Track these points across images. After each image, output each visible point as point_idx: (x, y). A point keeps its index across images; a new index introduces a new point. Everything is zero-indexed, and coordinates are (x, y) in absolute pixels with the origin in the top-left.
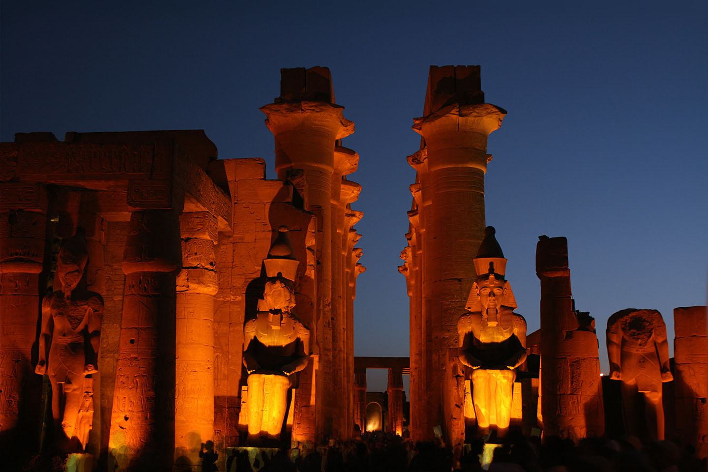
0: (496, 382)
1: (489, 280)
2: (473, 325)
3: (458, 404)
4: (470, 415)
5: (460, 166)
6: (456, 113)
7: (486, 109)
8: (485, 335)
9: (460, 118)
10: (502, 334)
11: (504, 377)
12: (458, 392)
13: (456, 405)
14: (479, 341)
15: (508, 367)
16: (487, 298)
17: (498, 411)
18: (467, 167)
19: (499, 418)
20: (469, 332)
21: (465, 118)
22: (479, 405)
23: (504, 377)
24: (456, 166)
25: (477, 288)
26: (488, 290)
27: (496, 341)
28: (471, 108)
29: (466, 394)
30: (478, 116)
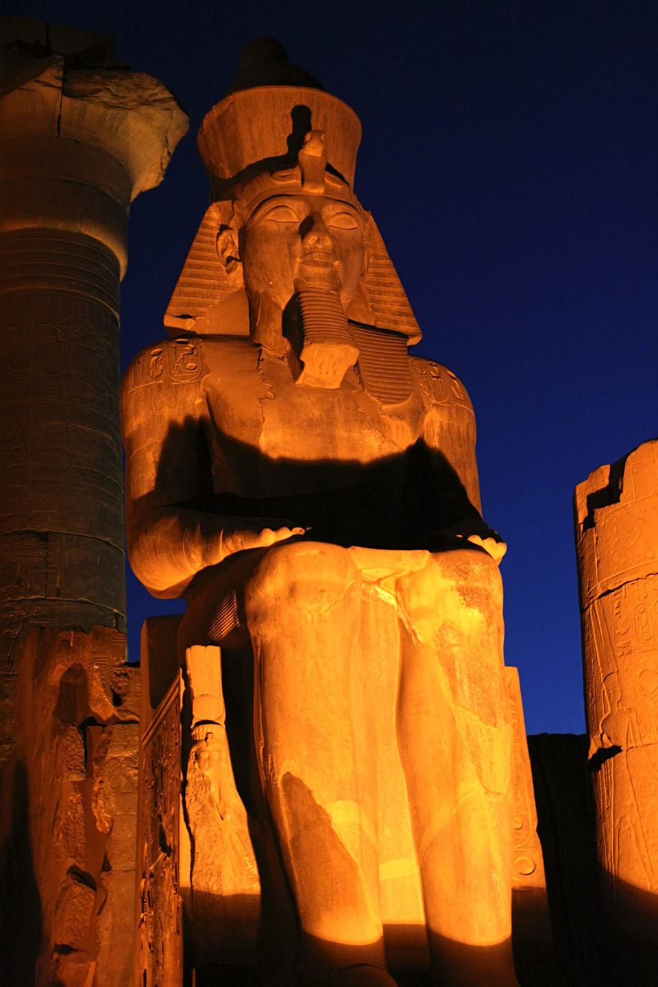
0: (407, 637)
1: (297, 171)
2: (216, 380)
3: (82, 867)
4: (228, 873)
5: (61, 226)
6: (54, 82)
7: (139, 87)
8: (287, 421)
9: (66, 99)
10: (377, 424)
11: (470, 595)
12: (87, 803)
13: (75, 872)
14: (250, 455)
15: (476, 540)
16: (290, 245)
17: (441, 816)
18: (80, 235)
19: (444, 875)
20: (189, 419)
21: (78, 103)
22: (310, 781)
23: (463, 592)
24: (47, 226)
25: (223, 228)
26: (294, 214)
27: (343, 453)
28: (98, 78)
29: (200, 732)
30: (112, 106)
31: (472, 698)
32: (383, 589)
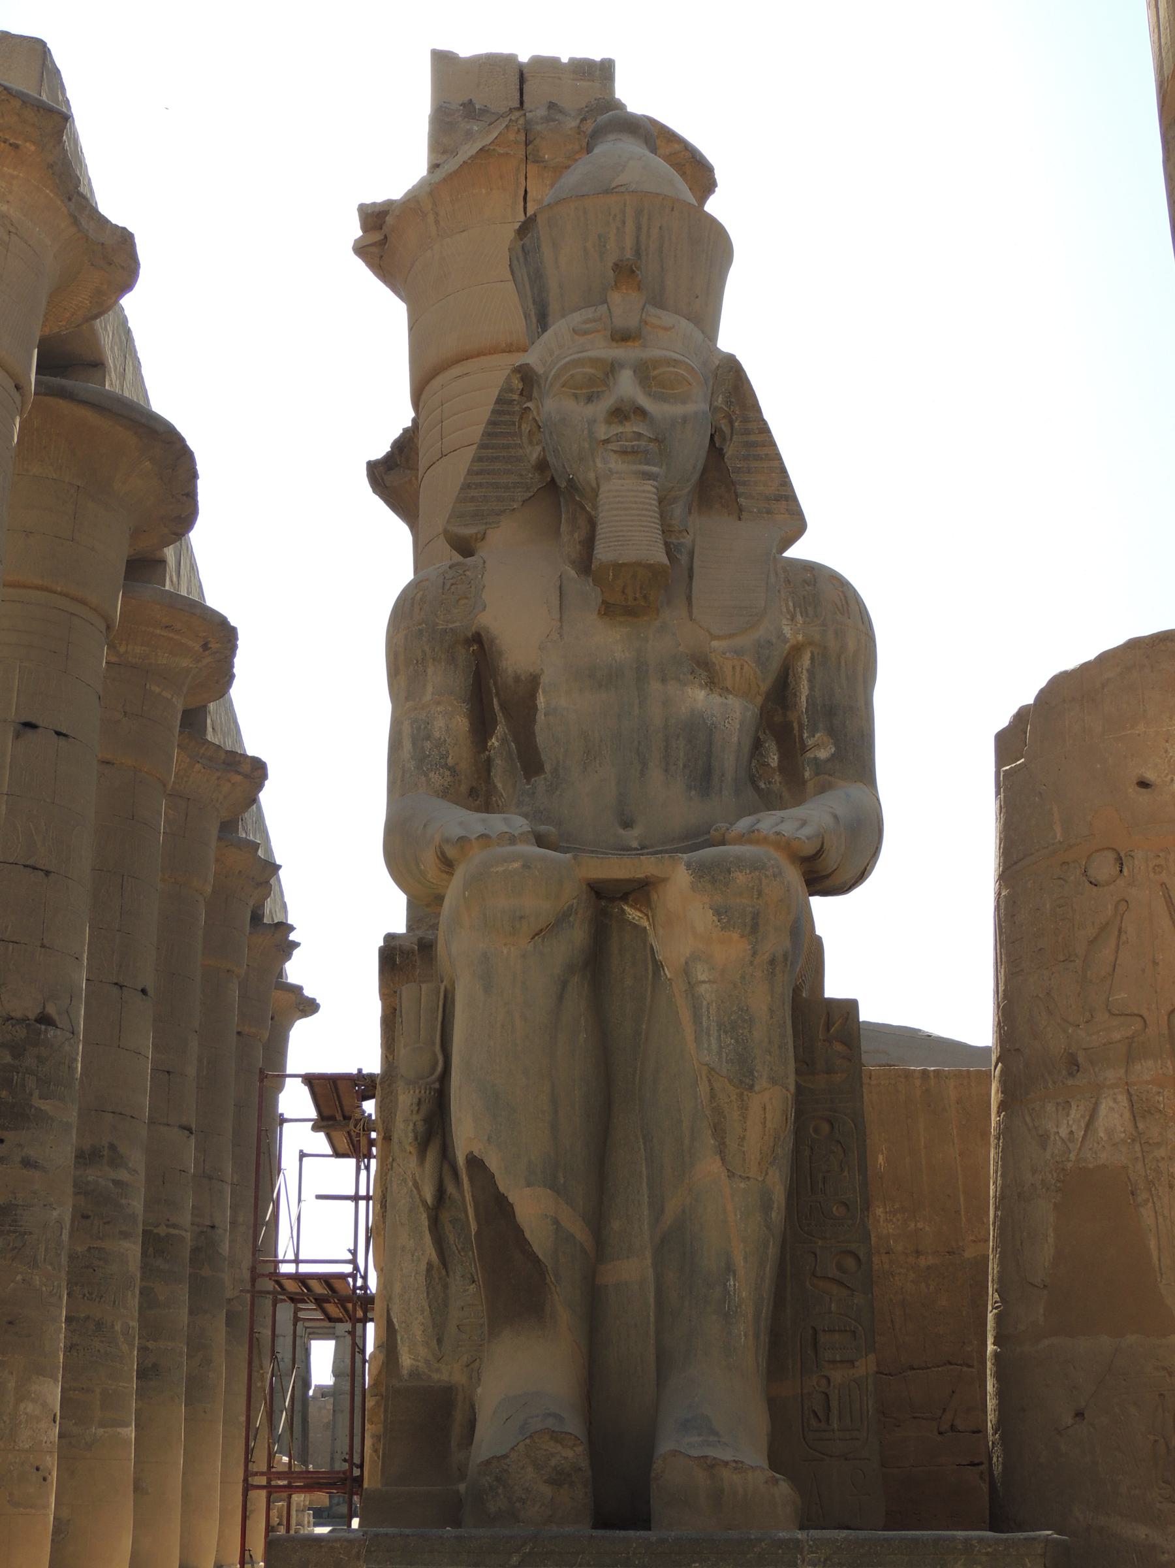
31: (719, 1053)
32: (631, 906)
